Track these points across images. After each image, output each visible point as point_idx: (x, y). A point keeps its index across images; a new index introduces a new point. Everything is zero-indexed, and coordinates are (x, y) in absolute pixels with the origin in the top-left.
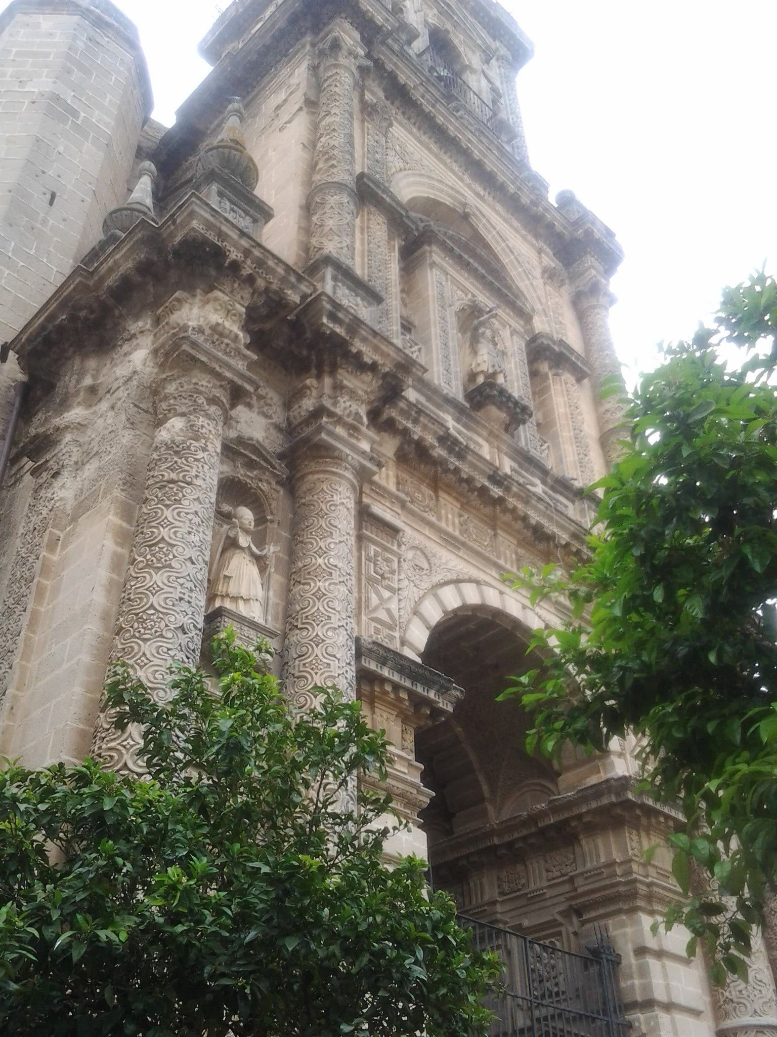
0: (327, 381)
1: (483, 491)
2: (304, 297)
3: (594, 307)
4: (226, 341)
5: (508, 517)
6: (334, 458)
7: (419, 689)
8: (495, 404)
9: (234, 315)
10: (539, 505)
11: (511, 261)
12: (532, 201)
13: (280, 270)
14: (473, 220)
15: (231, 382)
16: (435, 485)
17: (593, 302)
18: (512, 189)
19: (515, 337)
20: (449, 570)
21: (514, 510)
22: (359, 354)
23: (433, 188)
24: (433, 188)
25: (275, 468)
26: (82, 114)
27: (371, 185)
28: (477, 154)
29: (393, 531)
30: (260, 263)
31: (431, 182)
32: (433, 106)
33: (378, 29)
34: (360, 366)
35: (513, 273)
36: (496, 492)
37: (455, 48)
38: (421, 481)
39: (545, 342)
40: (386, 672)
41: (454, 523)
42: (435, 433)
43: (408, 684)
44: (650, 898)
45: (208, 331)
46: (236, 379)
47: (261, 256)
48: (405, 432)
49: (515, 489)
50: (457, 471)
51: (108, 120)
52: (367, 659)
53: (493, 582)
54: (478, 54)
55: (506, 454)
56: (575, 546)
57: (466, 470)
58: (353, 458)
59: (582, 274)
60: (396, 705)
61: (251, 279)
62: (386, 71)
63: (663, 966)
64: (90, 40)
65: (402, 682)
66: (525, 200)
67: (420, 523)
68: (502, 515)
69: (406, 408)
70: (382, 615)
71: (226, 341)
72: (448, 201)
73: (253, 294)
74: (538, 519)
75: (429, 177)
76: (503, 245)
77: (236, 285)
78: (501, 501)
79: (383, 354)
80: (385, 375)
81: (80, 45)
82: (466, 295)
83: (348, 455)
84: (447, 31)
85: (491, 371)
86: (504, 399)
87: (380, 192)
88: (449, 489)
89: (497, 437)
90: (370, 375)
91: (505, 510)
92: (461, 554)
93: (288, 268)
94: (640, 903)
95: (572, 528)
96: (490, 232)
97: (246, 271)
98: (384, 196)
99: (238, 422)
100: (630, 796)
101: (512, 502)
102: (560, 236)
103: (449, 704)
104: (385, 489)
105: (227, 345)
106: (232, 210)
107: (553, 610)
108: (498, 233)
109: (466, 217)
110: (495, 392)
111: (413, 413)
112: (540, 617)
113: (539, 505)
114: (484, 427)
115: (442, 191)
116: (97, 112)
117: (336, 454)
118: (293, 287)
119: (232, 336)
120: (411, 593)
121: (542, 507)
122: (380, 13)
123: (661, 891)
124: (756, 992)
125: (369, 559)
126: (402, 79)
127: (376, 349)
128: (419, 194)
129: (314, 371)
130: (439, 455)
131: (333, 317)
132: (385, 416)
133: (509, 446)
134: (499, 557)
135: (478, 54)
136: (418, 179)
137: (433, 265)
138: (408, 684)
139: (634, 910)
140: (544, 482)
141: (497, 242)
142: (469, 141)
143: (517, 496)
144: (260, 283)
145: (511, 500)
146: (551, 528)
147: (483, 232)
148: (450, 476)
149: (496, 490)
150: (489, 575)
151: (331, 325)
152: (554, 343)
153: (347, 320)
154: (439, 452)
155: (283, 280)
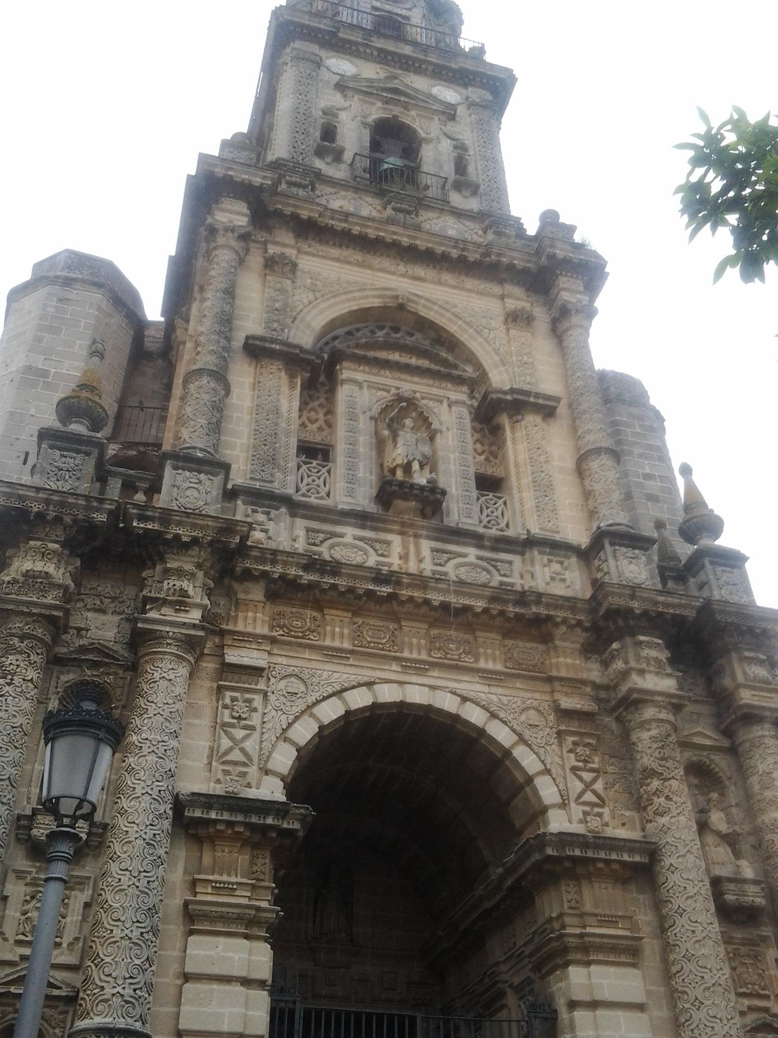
0: (159, 568)
1: (370, 594)
2: (110, 513)
3: (567, 330)
4: (40, 580)
5: (409, 607)
6: (157, 638)
7: (254, 819)
8: (400, 498)
9: (49, 554)
10: (439, 586)
11: (460, 327)
12: (482, 255)
13: (82, 502)
14: (411, 307)
15: (40, 615)
16: (319, 606)
17: (566, 324)
18: (455, 253)
19: (454, 408)
20: (330, 684)
21: (411, 599)
22: (177, 537)
23: (354, 299)
24: (354, 299)
25: (119, 660)
26: (53, 371)
27: (258, 343)
28: (405, 241)
29: (257, 672)
30: (62, 504)
31: (350, 296)
32: (346, 221)
33: (261, 188)
34: (181, 546)
35: (463, 338)
36: (386, 590)
37: (409, 127)
38: (305, 606)
39: (494, 396)
40: (213, 815)
41: (342, 636)
42: (298, 564)
43: (240, 818)
44: (585, 949)
45: (21, 579)
46: (43, 611)
47: (61, 499)
48: (265, 575)
49: (406, 581)
50: (334, 587)
51: (77, 364)
52: (191, 809)
53: (393, 676)
54: (436, 118)
55: (428, 537)
56: (496, 608)
57: (342, 583)
58: (174, 633)
59: (555, 299)
60: (237, 837)
61: (58, 520)
62: (287, 216)
63: (595, 1017)
64: (61, 300)
65: (233, 819)
66: (472, 257)
67: (299, 649)
68: (400, 608)
69: (259, 554)
70: (236, 755)
71: (40, 580)
72: (376, 303)
73: (65, 529)
74: (442, 598)
75: (346, 293)
76: (448, 315)
77: (47, 529)
78: (392, 597)
79: (202, 528)
80: (211, 543)
81: (51, 310)
82: (388, 391)
83: (168, 632)
84: (395, 117)
85: (405, 462)
86: (407, 490)
87: (268, 345)
88: (333, 605)
89: (411, 526)
90: (196, 549)
91: (402, 603)
92: (351, 662)
93: (87, 498)
94: (572, 956)
95: (487, 592)
96: (431, 309)
97: (52, 514)
98: (273, 346)
99: (87, 630)
100: (550, 851)
101: (405, 593)
102: (525, 271)
103: (296, 823)
104: (249, 635)
105: (41, 583)
106: (62, 456)
107: (477, 679)
108: (440, 306)
109: (401, 307)
110: (394, 488)
111: (268, 556)
112: (454, 693)
113: (439, 586)
114: (393, 522)
115: (367, 297)
116: (67, 362)
117: (157, 635)
118: (98, 510)
119: (43, 574)
121: (444, 586)
122: (256, 176)
123: (610, 941)
124: (708, 1030)
125: (225, 707)
126: (304, 214)
127: (194, 526)
128: (338, 314)
129: (149, 563)
130: (309, 581)
131: (142, 518)
132: (239, 569)
133: (428, 529)
134: (402, 651)
135: (436, 118)
136: (332, 301)
137: (343, 382)
138: (240, 818)
139: (567, 964)
140: (480, 547)
141: (441, 315)
142: (394, 233)
143: (409, 586)
144: (68, 519)
145: (404, 592)
146: (461, 601)
147: (423, 312)
148: (331, 593)
149: (384, 589)
150: (392, 671)
151: (142, 525)
152: (505, 393)
153: (157, 515)
154: (307, 577)
155: (88, 508)
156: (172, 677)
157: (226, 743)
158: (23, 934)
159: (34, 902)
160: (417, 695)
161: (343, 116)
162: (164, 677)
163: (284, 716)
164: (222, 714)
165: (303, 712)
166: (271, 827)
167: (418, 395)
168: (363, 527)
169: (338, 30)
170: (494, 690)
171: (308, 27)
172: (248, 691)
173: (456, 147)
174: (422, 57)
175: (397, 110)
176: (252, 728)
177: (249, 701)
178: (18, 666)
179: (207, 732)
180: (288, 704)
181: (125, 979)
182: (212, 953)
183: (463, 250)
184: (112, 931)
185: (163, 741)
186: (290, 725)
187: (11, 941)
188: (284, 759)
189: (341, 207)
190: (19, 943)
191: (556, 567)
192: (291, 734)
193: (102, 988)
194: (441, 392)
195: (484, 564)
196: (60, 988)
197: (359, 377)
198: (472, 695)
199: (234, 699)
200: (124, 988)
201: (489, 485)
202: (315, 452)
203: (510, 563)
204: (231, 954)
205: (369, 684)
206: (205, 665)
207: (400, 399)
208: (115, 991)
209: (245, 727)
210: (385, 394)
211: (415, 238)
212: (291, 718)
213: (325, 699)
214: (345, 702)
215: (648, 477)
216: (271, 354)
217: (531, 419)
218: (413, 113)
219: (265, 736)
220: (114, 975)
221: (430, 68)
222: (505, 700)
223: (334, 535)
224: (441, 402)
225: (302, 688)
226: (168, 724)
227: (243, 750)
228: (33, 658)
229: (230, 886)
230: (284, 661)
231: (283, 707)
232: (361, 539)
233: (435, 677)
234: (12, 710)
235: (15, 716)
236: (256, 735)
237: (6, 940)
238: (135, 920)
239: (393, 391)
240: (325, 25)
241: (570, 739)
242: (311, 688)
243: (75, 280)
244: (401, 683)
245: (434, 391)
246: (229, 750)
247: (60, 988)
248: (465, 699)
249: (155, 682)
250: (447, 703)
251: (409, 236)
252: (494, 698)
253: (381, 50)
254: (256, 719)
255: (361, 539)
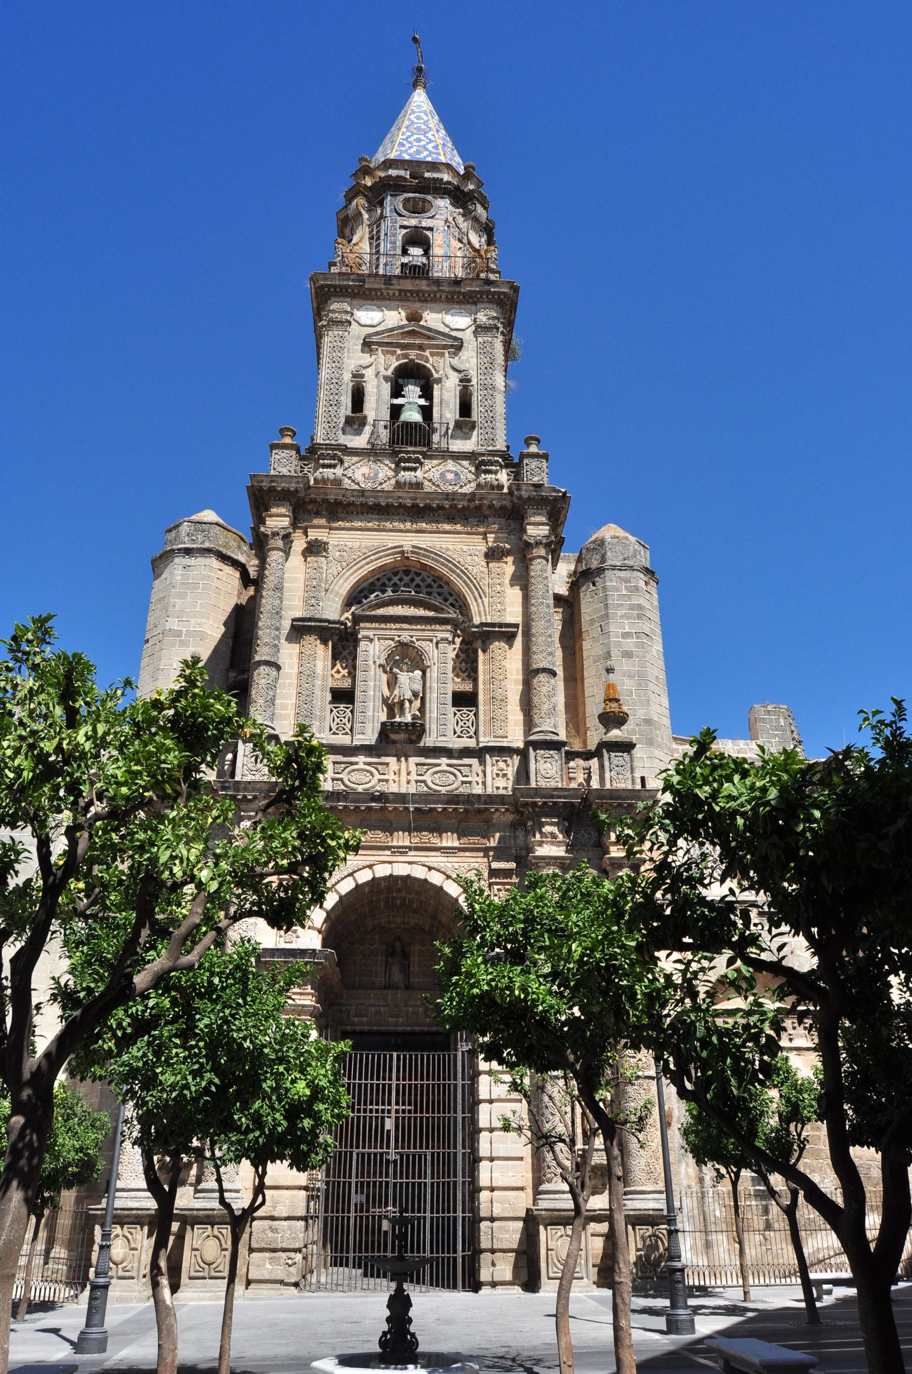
12: (469, 501)
18: (447, 504)
28: (409, 503)
82: (393, 640)
115: (381, 558)
150: (386, 855)
160: (401, 870)
161: (369, 374)
167: (414, 639)
168: (371, 756)
169: (364, 282)
170: (450, 859)
171: (339, 286)
173: (461, 381)
174: (435, 289)
175: (413, 354)
183: (453, 500)
189: (386, 427)
191: (502, 765)
194: (430, 633)
195: (452, 769)
197: (370, 633)
198: (435, 865)
201: (465, 700)
202: (343, 696)
203: (470, 766)
205: (370, 867)
207: (401, 644)
210: (391, 642)
211: (416, 499)
214: (355, 880)
215: (626, 635)
216: (309, 630)
217: (497, 646)
218: (427, 353)
221: (444, 297)
222: (456, 865)
223: (352, 764)
224: (431, 641)
232: (369, 764)
233: (412, 856)
239: (397, 639)
240: (353, 280)
241: (496, 887)
243: (192, 549)
244: (390, 863)
245: (426, 633)
248: (430, 868)
250: (419, 873)
251: (411, 498)
252: (449, 865)
253: (400, 291)
255: (369, 764)
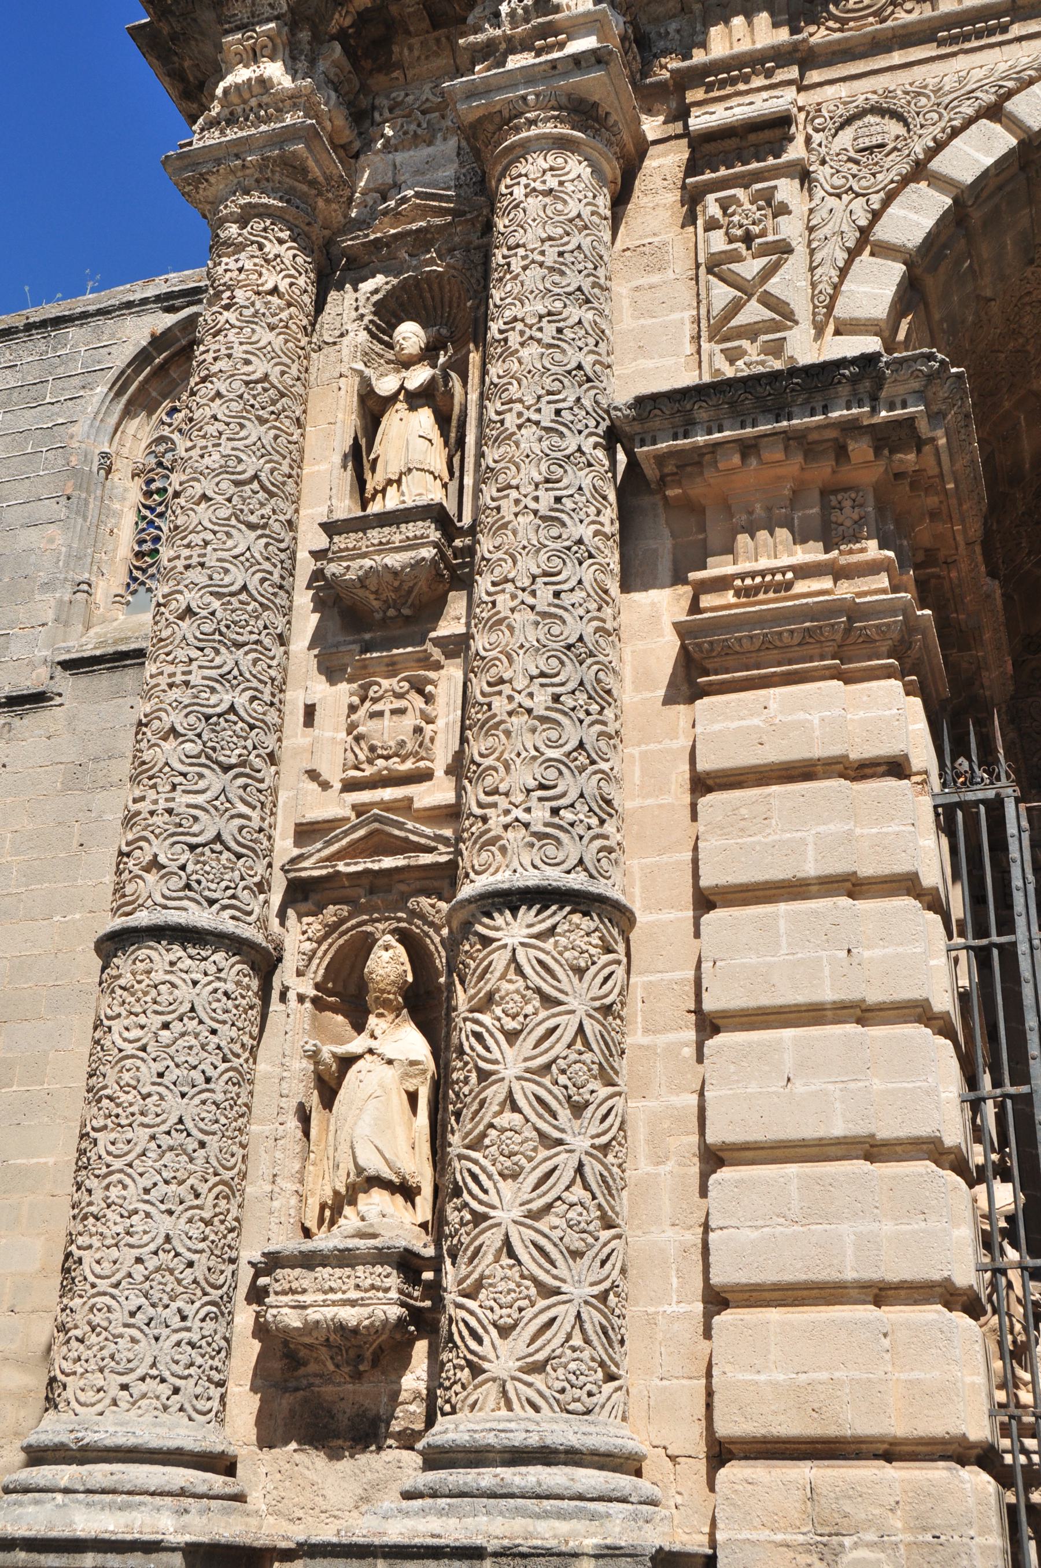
29: (775, 129)
70: (754, 312)
120: (843, 216)
156: (552, 183)
157: (722, 294)
158: (357, 768)
159: (367, 704)
162: (534, 190)
163: (859, 203)
164: (707, 241)
165: (906, 181)
166: (851, 427)
172: (758, 176)
176: (784, 249)
177: (767, 197)
178: (240, 270)
179: (685, 293)
180: (865, 172)
181: (528, 791)
182: (756, 721)
184: (489, 705)
185: (550, 314)
186: (876, 216)
187: (338, 786)
188: (874, 288)
190: (350, 786)
192: (882, 232)
193: (485, 819)
196: (435, 849)
199: (724, 205)
200: (528, 810)
204: (802, 716)
206: (655, 163)
208: (509, 819)
209: (766, 250)
212: (876, 203)
213: (955, 132)
219: (818, 257)
220: (503, 788)
225: (895, 128)
226: (557, 278)
227: (769, 301)
228: (272, 249)
229: (779, 577)
230: (842, 90)
231: (852, 182)
234: (238, 352)
235: (247, 362)
236: (795, 266)
237: (325, 786)
238: (535, 672)
242: (920, 120)
246: (735, 308)
247: (435, 849)
249: (517, 206)
254: (790, 228)
